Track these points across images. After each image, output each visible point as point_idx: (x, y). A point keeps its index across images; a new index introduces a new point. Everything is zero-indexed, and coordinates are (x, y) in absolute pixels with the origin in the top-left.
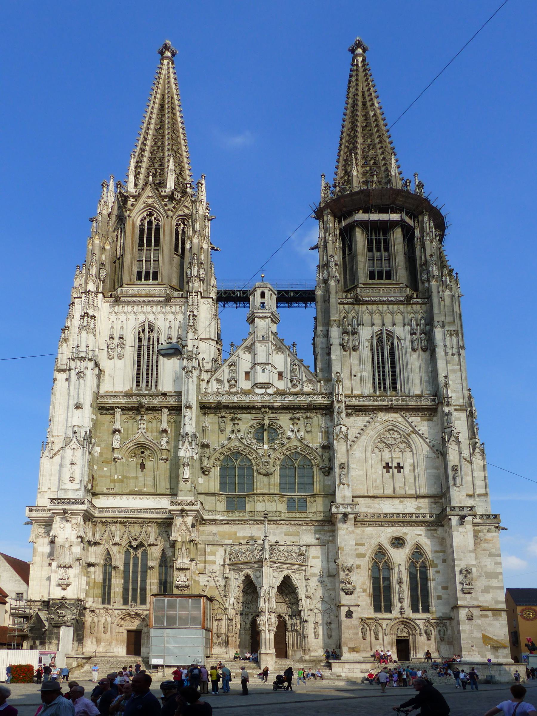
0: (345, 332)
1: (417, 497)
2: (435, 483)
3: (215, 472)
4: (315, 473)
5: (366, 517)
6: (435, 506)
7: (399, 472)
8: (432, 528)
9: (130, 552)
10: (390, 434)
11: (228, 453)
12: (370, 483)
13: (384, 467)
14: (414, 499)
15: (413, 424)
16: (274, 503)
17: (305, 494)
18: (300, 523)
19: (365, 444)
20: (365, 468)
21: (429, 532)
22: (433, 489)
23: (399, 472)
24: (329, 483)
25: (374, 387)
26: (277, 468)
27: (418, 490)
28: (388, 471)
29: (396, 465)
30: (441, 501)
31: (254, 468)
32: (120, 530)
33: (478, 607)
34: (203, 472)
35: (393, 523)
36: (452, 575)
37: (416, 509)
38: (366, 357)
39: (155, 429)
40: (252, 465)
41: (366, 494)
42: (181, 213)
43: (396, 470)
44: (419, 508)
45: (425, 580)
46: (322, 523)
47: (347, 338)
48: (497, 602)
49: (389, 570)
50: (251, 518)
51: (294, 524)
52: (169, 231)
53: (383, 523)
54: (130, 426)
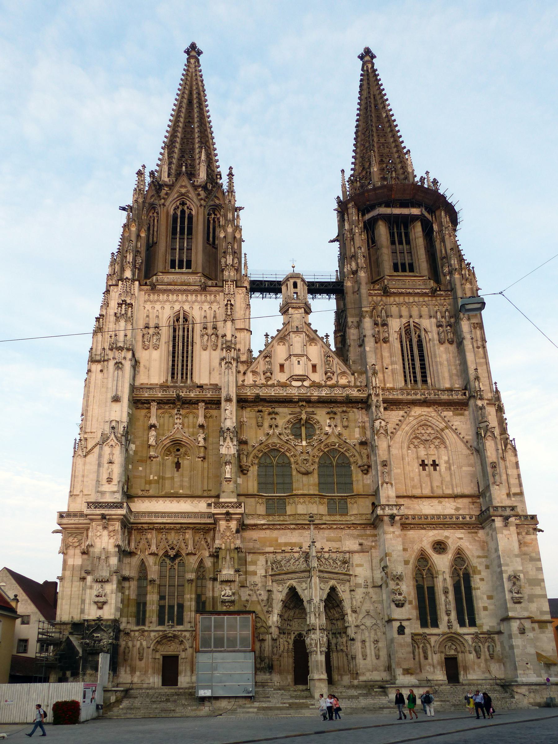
0: (376, 324)
1: (456, 497)
2: (472, 481)
3: (254, 471)
4: (354, 472)
5: (407, 519)
6: (473, 506)
7: (435, 469)
8: (473, 531)
11: (266, 451)
12: (408, 481)
13: (421, 465)
14: (453, 499)
15: (446, 419)
16: (315, 505)
17: (345, 495)
20: (402, 466)
21: (470, 535)
22: (470, 488)
23: (435, 469)
24: (369, 482)
25: (406, 381)
26: (316, 466)
28: (424, 469)
30: (478, 501)
31: (293, 466)
33: (528, 618)
34: (242, 471)
35: (434, 526)
36: (498, 583)
37: (455, 509)
38: (396, 349)
39: (191, 425)
40: (290, 463)
41: (405, 494)
42: (212, 203)
44: (457, 509)
45: (469, 589)
46: (363, 526)
47: (377, 329)
48: (543, 613)
49: (433, 578)
50: (292, 522)
51: (336, 528)
52: (202, 220)
53: (425, 526)
54: (166, 421)
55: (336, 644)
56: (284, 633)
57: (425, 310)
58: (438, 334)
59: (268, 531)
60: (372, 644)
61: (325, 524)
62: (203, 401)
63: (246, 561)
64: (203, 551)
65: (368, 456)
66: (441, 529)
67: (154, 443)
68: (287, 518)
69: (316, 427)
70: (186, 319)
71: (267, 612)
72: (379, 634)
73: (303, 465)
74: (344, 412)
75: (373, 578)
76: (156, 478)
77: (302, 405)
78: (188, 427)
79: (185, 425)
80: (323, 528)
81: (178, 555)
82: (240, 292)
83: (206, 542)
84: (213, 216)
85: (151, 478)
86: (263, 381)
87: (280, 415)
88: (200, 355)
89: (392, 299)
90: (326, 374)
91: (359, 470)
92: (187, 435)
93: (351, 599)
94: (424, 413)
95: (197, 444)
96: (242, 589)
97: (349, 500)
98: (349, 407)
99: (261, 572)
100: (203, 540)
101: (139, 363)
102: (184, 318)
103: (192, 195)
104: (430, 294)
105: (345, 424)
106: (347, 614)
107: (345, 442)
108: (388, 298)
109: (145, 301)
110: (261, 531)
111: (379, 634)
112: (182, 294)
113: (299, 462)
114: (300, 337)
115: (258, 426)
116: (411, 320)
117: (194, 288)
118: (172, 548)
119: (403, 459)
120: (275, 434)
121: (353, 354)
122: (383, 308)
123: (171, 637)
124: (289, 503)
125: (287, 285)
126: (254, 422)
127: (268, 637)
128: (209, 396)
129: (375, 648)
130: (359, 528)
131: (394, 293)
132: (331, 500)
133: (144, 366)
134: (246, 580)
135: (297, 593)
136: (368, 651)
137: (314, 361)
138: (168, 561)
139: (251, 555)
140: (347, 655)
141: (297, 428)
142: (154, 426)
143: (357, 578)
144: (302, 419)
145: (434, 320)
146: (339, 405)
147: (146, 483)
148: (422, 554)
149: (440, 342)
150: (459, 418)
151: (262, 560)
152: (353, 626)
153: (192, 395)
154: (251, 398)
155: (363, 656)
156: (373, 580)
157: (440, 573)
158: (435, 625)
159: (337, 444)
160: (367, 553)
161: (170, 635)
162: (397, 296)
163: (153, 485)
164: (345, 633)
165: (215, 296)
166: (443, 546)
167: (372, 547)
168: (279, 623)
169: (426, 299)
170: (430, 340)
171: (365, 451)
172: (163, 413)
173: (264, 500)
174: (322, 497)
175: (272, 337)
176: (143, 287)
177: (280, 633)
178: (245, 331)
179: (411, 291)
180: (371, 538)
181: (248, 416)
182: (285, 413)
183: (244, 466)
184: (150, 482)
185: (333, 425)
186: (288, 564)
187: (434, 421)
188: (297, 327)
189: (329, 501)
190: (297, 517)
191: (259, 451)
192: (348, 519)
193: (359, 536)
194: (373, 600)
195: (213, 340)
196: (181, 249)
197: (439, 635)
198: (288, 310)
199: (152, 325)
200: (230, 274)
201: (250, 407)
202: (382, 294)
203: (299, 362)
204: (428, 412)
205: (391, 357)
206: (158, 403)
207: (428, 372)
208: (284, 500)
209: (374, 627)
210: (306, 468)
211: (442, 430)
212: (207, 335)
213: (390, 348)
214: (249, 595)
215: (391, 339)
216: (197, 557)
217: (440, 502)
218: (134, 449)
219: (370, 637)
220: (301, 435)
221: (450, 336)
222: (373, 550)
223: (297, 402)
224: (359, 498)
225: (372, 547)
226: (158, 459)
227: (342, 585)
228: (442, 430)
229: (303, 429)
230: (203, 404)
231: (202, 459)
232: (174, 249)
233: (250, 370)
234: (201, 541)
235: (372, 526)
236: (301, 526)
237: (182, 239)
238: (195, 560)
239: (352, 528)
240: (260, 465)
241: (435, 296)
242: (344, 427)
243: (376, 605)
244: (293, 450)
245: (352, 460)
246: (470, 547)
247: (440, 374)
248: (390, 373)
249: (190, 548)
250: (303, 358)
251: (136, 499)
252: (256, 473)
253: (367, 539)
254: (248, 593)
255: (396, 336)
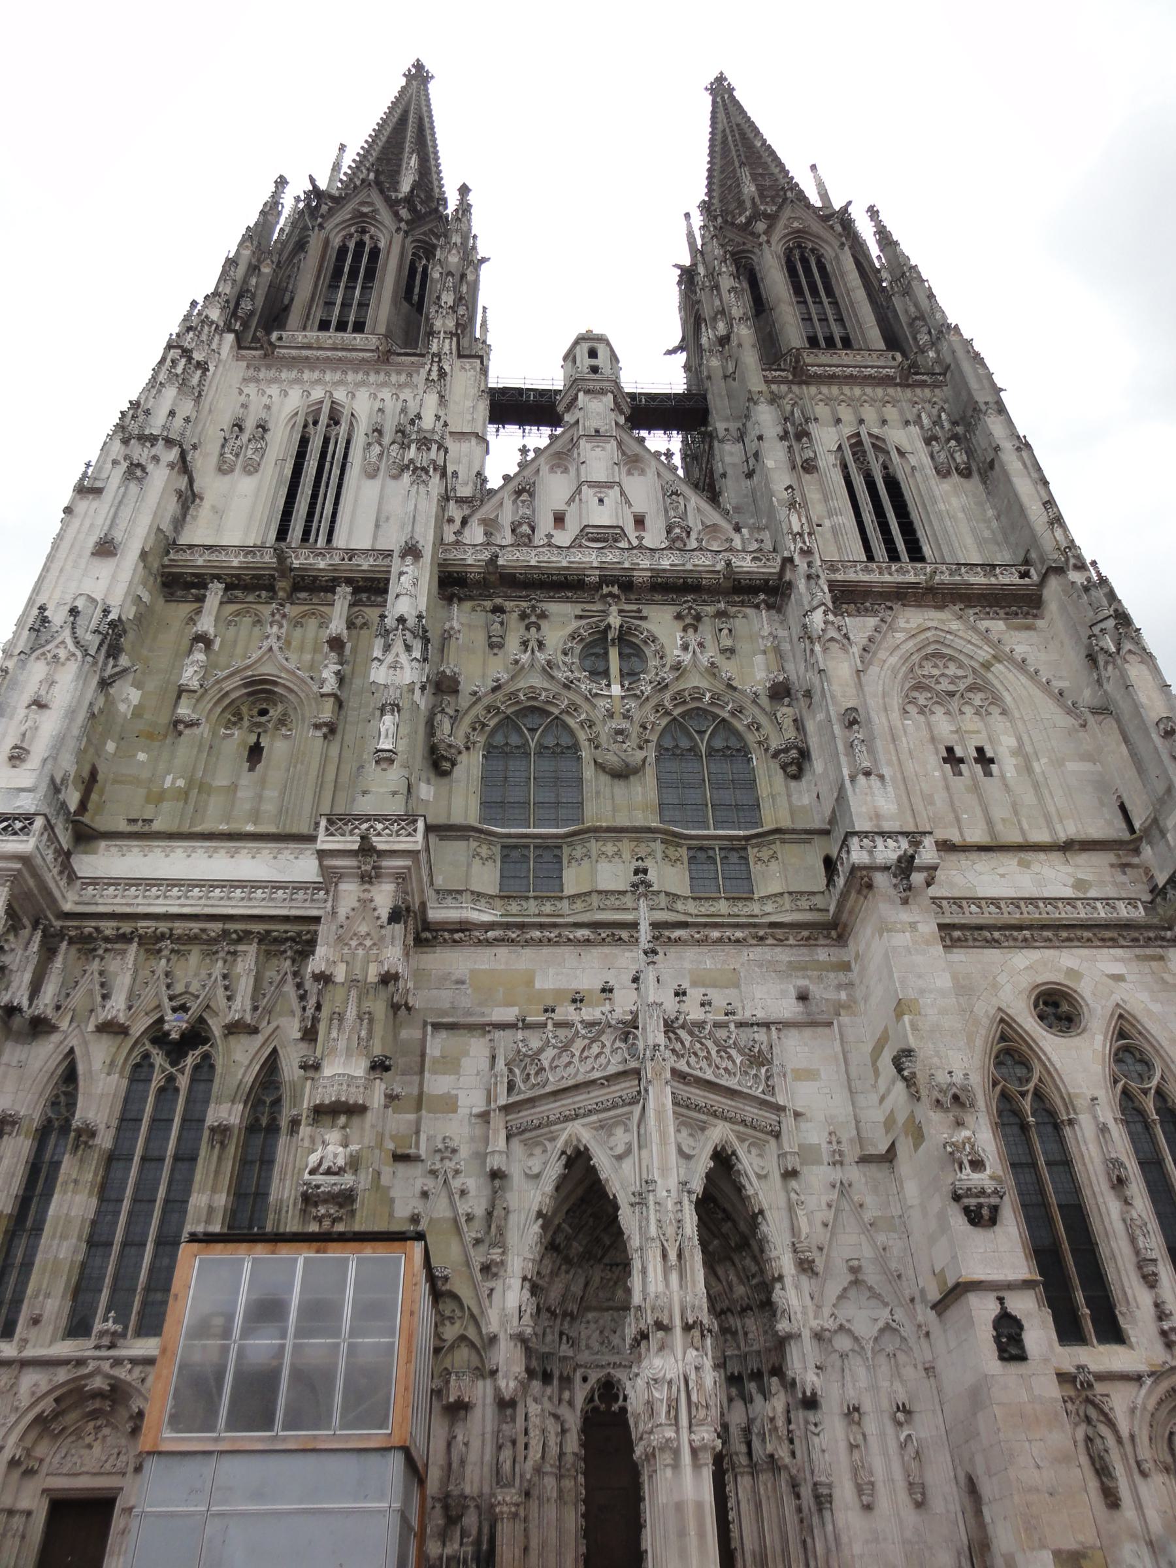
1: (1067, 847)
2: (1102, 804)
3: (470, 766)
6: (1123, 879)
8: (1148, 951)
9: (152, 1066)
10: (935, 666)
11: (509, 711)
14: (1059, 854)
17: (741, 833)
18: (739, 934)
19: (881, 689)
20: (894, 758)
21: (1145, 967)
26: (651, 753)
27: (1058, 827)
29: (976, 755)
30: (1136, 860)
31: (586, 754)
32: (136, 971)
35: (1027, 933)
37: (1073, 886)
40: (575, 747)
43: (978, 768)
44: (1079, 884)
46: (805, 933)
51: (720, 940)
53: (996, 934)
55: (747, 1431)
56: (547, 1378)
57: (891, 412)
58: (932, 457)
59: (502, 951)
60: (890, 1429)
61: (684, 925)
62: (349, 581)
63: (423, 1055)
64: (283, 1021)
65: (799, 724)
66: (1049, 944)
67: (195, 684)
68: (566, 902)
69: (649, 651)
70: (334, 420)
71: (486, 1269)
72: (909, 1372)
73: (614, 747)
74: (721, 614)
75: (857, 1122)
76: (181, 783)
77: (611, 595)
78: (302, 649)
79: (294, 644)
80: (678, 940)
81: (196, 1036)
82: (468, 367)
83: (299, 986)
84: (424, 262)
85: (168, 783)
86: (508, 539)
87: (552, 618)
88: (359, 488)
89: (813, 389)
90: (668, 533)
91: (775, 766)
92: (291, 666)
93: (791, 1209)
94: (930, 624)
95: (315, 688)
96: (401, 1168)
97: (752, 852)
98: (734, 604)
99: (472, 1100)
100: (289, 977)
101: (202, 499)
102: (331, 418)
103: (385, 215)
104: (898, 380)
105: (727, 642)
106: (780, 1278)
107: (730, 686)
108: (804, 387)
109: (244, 380)
110: (479, 950)
111: (909, 1372)
112: (334, 370)
113: (603, 740)
114: (604, 449)
115: (492, 646)
116: (863, 431)
117: (361, 354)
118: (183, 1008)
119: (894, 740)
120: (538, 667)
121: (732, 491)
122: (793, 405)
123: (98, 1394)
124: (571, 858)
125: (575, 357)
126: (480, 638)
127: (481, 1394)
128: (365, 567)
129: (903, 1446)
130: (791, 941)
131: (816, 375)
132: (700, 853)
133: (213, 507)
134: (417, 1133)
135: (592, 1171)
136: (878, 1464)
137: (638, 508)
138: (159, 1059)
139: (443, 1034)
140: (794, 1486)
141: (597, 655)
142: (203, 640)
143: (804, 1125)
144: (609, 627)
145: (914, 430)
146: (705, 597)
147: (148, 800)
148: (1003, 1038)
149: (938, 472)
150: (1024, 635)
151: (477, 1049)
152: (806, 1334)
153: (322, 564)
154: (474, 574)
155: (860, 1490)
156: (857, 1129)
157: (1081, 1103)
158: (1112, 1332)
159: (708, 695)
160: (827, 1030)
161: (98, 1383)
162: (823, 383)
163: (166, 806)
164: (778, 1371)
165: (410, 375)
166: (1065, 1007)
167: (839, 1008)
168: (527, 1318)
169: (891, 391)
170: (913, 468)
171: (785, 710)
172: (238, 614)
173: (497, 850)
174: (672, 839)
175: (537, 450)
176: (244, 352)
177: (530, 1372)
178: (474, 441)
179: (855, 372)
180: (832, 975)
181: (464, 620)
182: (566, 615)
183: (443, 746)
184: (159, 798)
185: (693, 644)
186: (565, 1059)
187: (959, 643)
188: (597, 431)
189: (692, 853)
190: (595, 900)
191: (488, 709)
192: (757, 911)
193: (795, 968)
194: (868, 1216)
195: (394, 454)
196: (346, 305)
197: (1138, 1378)
198: (576, 398)
199: (250, 425)
200: (443, 323)
201: (471, 598)
202: (791, 377)
203: (601, 501)
204: (942, 621)
205: (826, 500)
206: (228, 588)
207: (920, 534)
208: (557, 852)
209: (890, 1346)
210: (623, 755)
211: (987, 666)
212: (380, 445)
213: (821, 483)
214: (425, 1195)
215: (821, 463)
216: (259, 1039)
217: (1023, 864)
218: (135, 702)
219: (874, 1388)
220: (606, 673)
221: (960, 457)
222: (845, 1019)
223: (598, 587)
224: (783, 841)
225: (839, 1008)
226: (196, 731)
227: (754, 1151)
228: (987, 666)
229: (613, 654)
230: (349, 590)
231: (325, 730)
232: (330, 304)
233: (479, 515)
234: (283, 981)
235: (834, 934)
236: (608, 932)
237: (350, 288)
238: (252, 1051)
239: (770, 941)
240: (490, 751)
241: (908, 386)
242: (723, 651)
243: (881, 1238)
244: (585, 706)
245: (751, 738)
246: (1156, 1008)
247: (953, 538)
248: (829, 535)
249: (240, 1010)
250: (610, 492)
251: (103, 844)
252: (477, 772)
253: (820, 978)
254: (418, 1185)
255: (832, 459)
